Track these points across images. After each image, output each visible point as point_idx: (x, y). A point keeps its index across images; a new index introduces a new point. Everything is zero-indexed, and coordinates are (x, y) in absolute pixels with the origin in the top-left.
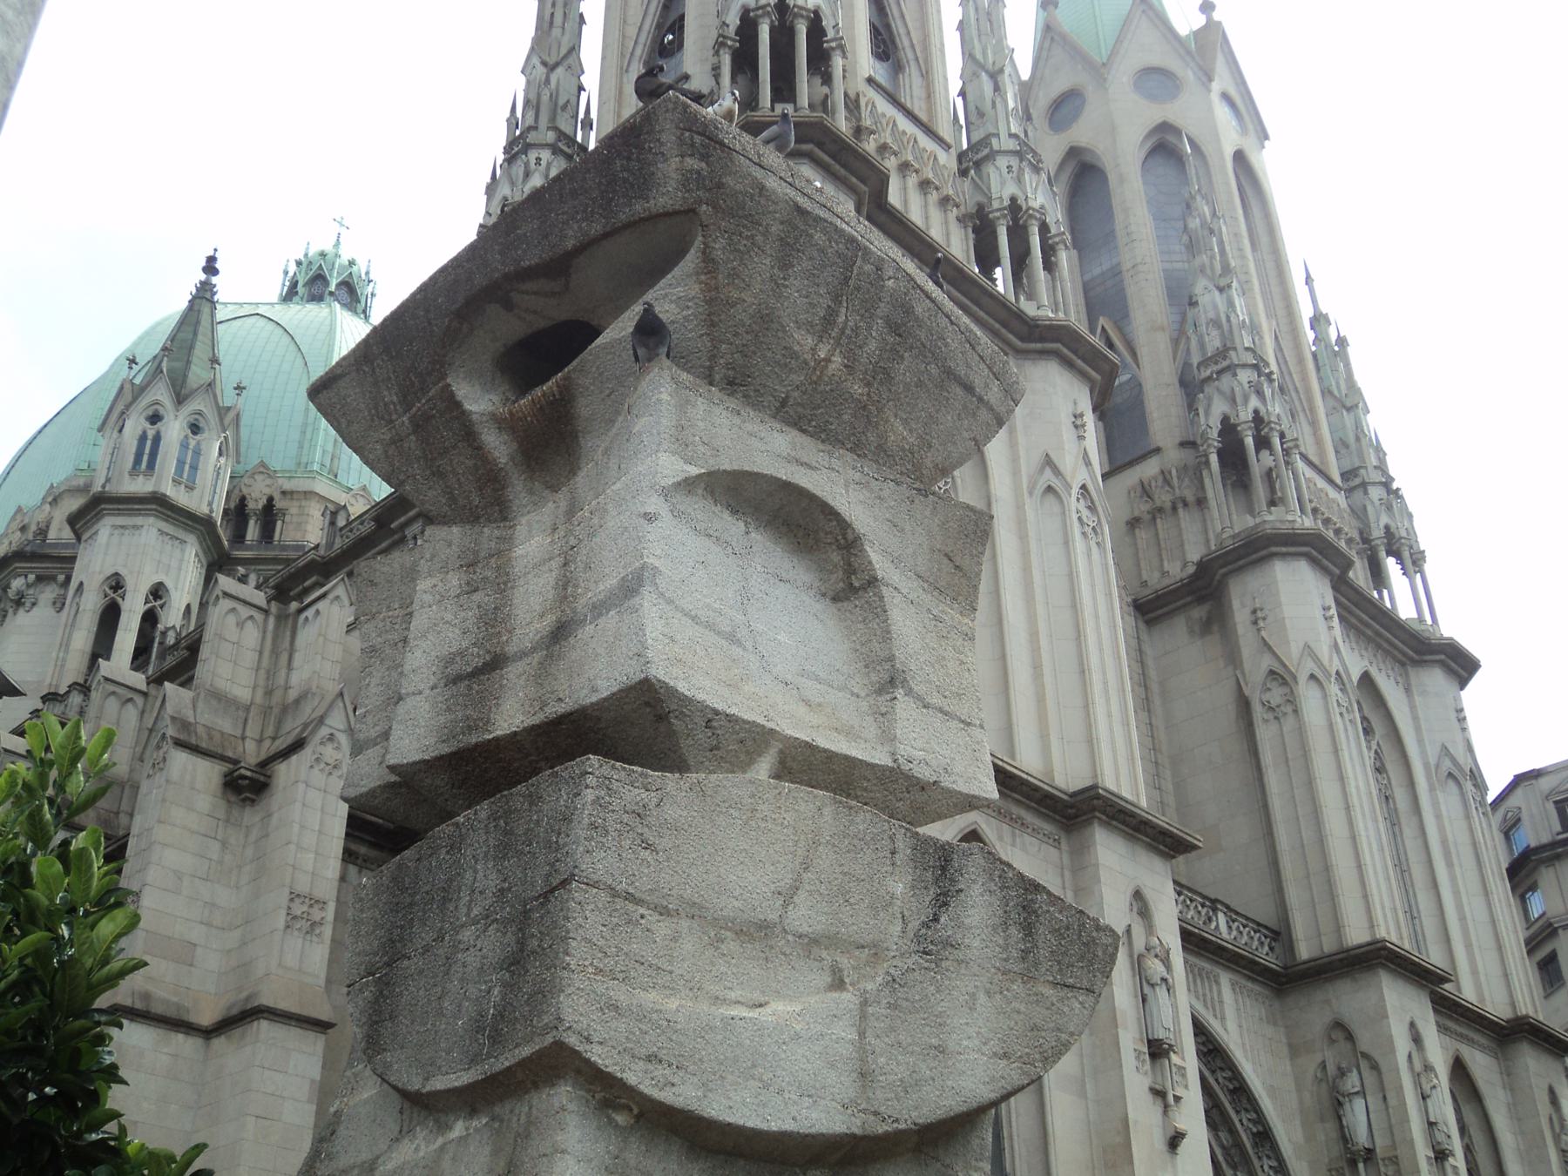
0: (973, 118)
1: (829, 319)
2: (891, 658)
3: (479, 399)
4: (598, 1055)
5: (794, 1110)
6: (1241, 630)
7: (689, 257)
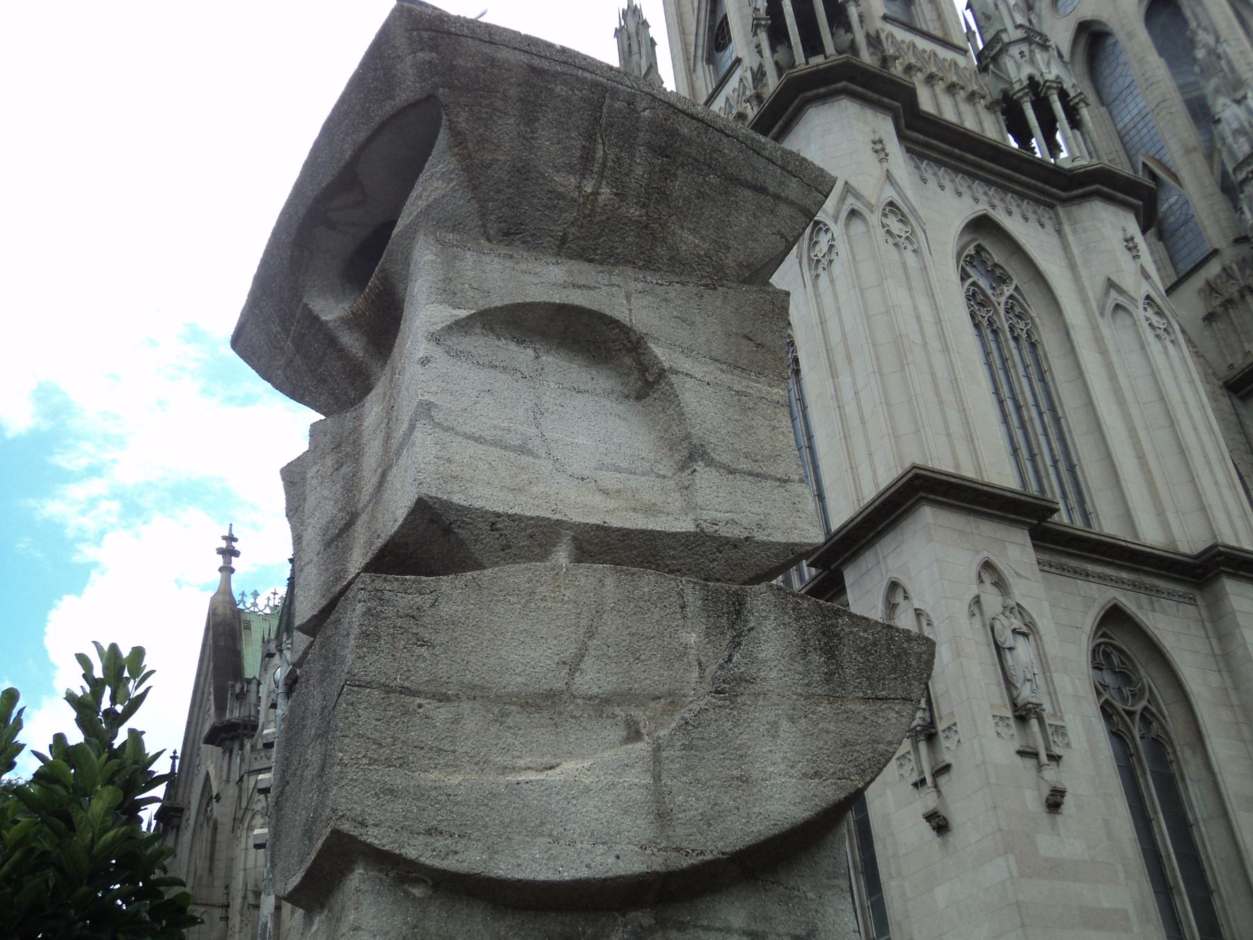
0: (982, 23)
1: (587, 157)
2: (688, 436)
3: (331, 310)
4: (374, 837)
5: (587, 860)
7: (440, 136)
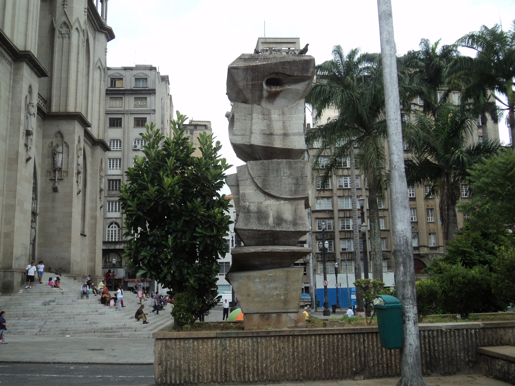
6: (58, 5)
